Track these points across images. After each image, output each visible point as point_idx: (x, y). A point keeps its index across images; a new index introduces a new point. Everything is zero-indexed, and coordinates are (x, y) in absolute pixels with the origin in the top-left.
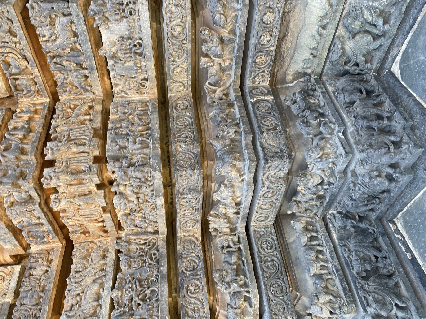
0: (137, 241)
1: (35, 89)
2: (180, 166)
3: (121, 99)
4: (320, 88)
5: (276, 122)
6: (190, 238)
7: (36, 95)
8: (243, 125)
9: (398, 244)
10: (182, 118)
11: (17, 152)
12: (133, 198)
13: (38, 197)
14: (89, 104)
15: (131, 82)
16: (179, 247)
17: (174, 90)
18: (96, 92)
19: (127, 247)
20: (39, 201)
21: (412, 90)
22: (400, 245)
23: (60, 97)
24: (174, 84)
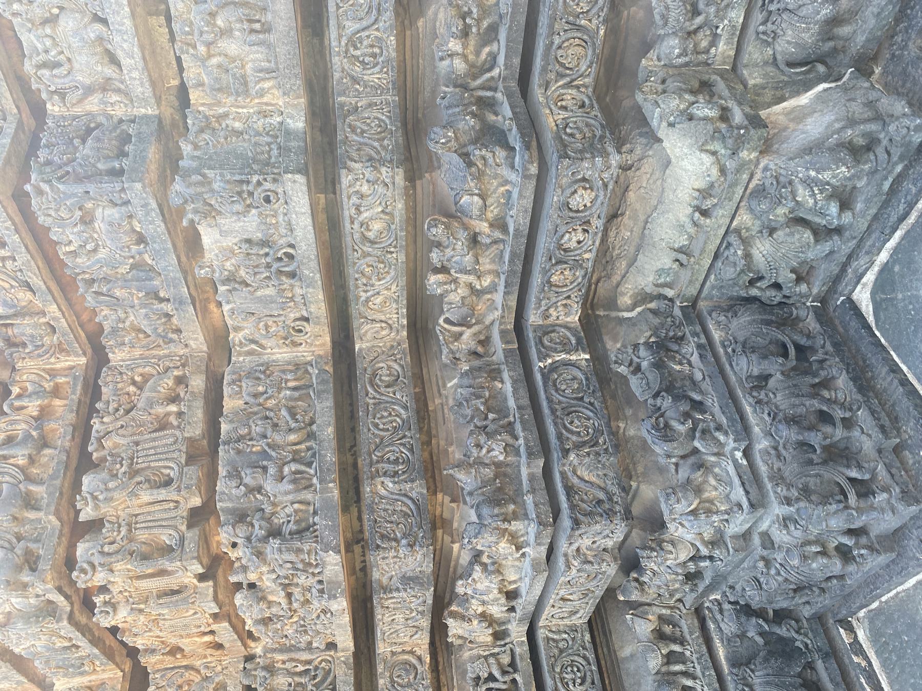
0: (288, 665)
1: (52, 341)
2: (383, 537)
3: (248, 358)
4: (695, 334)
5: (596, 424)
6: (406, 657)
7: (54, 353)
8: (524, 430)
9: (858, 679)
10: (386, 409)
11: (15, 506)
12: (279, 597)
13: (65, 603)
14: (176, 373)
15: (270, 323)
16: (381, 682)
17: (369, 336)
18: (192, 343)
19: (268, 682)
20: (68, 609)
21: (898, 355)
22: (863, 680)
23: (110, 355)
24: (369, 326)
